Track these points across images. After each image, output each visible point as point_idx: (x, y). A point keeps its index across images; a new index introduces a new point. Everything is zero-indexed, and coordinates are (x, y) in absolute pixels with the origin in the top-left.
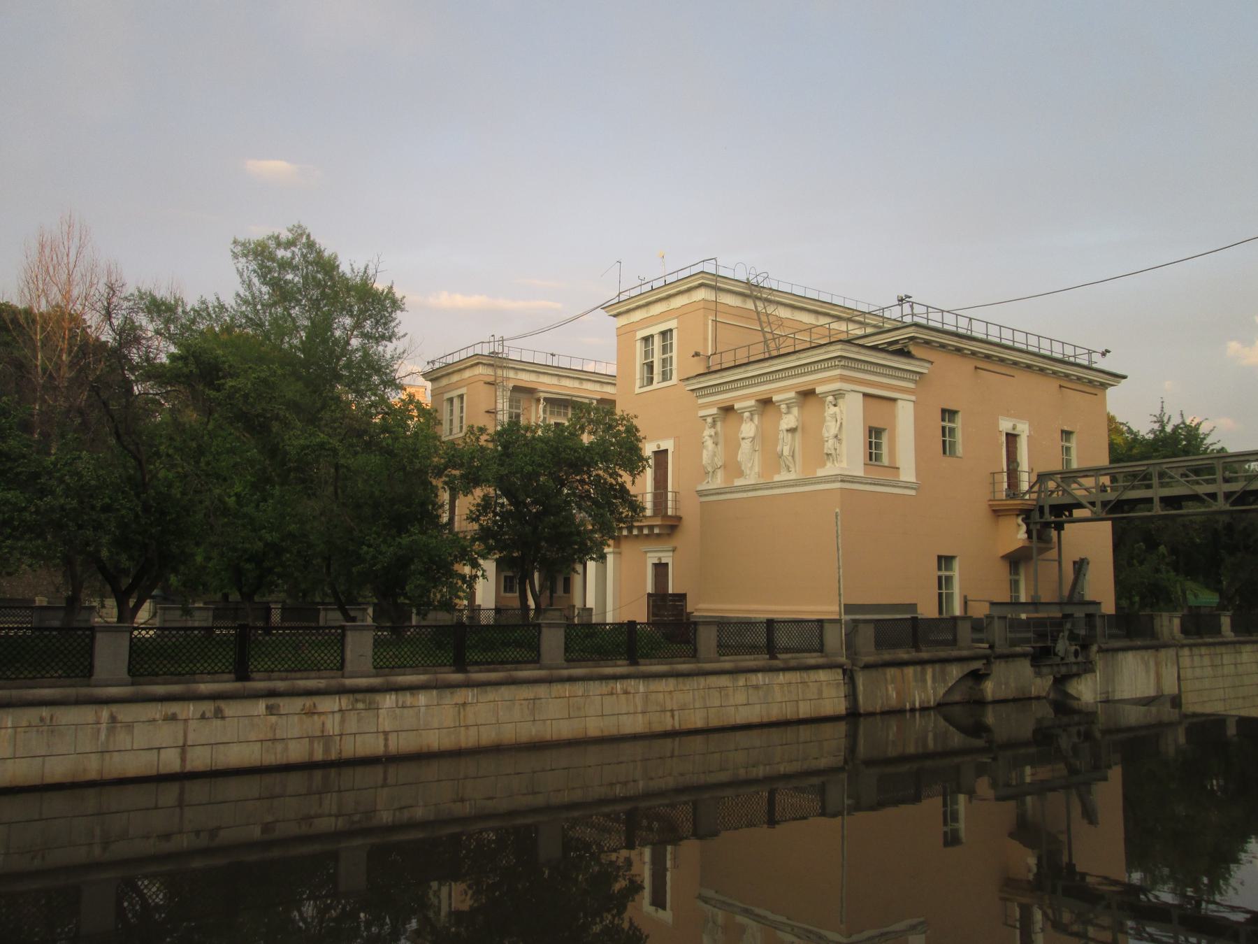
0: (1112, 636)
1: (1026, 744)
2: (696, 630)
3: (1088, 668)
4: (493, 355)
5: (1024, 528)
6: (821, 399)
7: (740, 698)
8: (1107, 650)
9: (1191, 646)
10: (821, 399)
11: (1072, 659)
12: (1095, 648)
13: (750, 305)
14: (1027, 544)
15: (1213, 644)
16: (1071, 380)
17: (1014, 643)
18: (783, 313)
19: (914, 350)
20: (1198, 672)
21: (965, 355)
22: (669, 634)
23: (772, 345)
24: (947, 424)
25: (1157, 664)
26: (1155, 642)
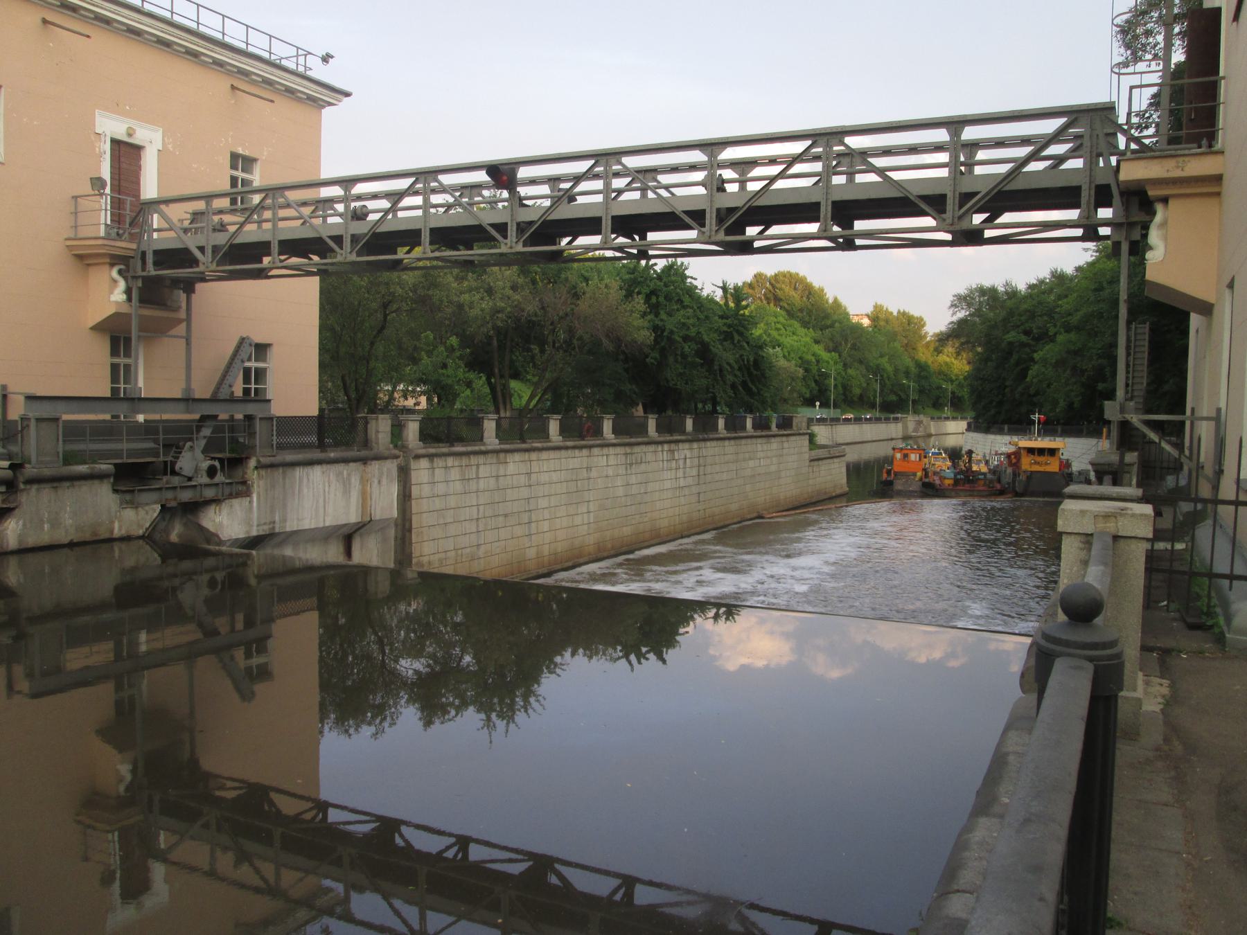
0: (281, 447)
1: (102, 607)
3: (242, 490)
5: (122, 285)
8: (272, 466)
9: (431, 457)
11: (205, 479)
12: (252, 463)
14: (125, 309)
15: (468, 454)
16: (254, 83)
17: (69, 459)
20: (441, 489)
21: (299, 100)
24: (240, 174)
25: (364, 481)
26: (364, 453)
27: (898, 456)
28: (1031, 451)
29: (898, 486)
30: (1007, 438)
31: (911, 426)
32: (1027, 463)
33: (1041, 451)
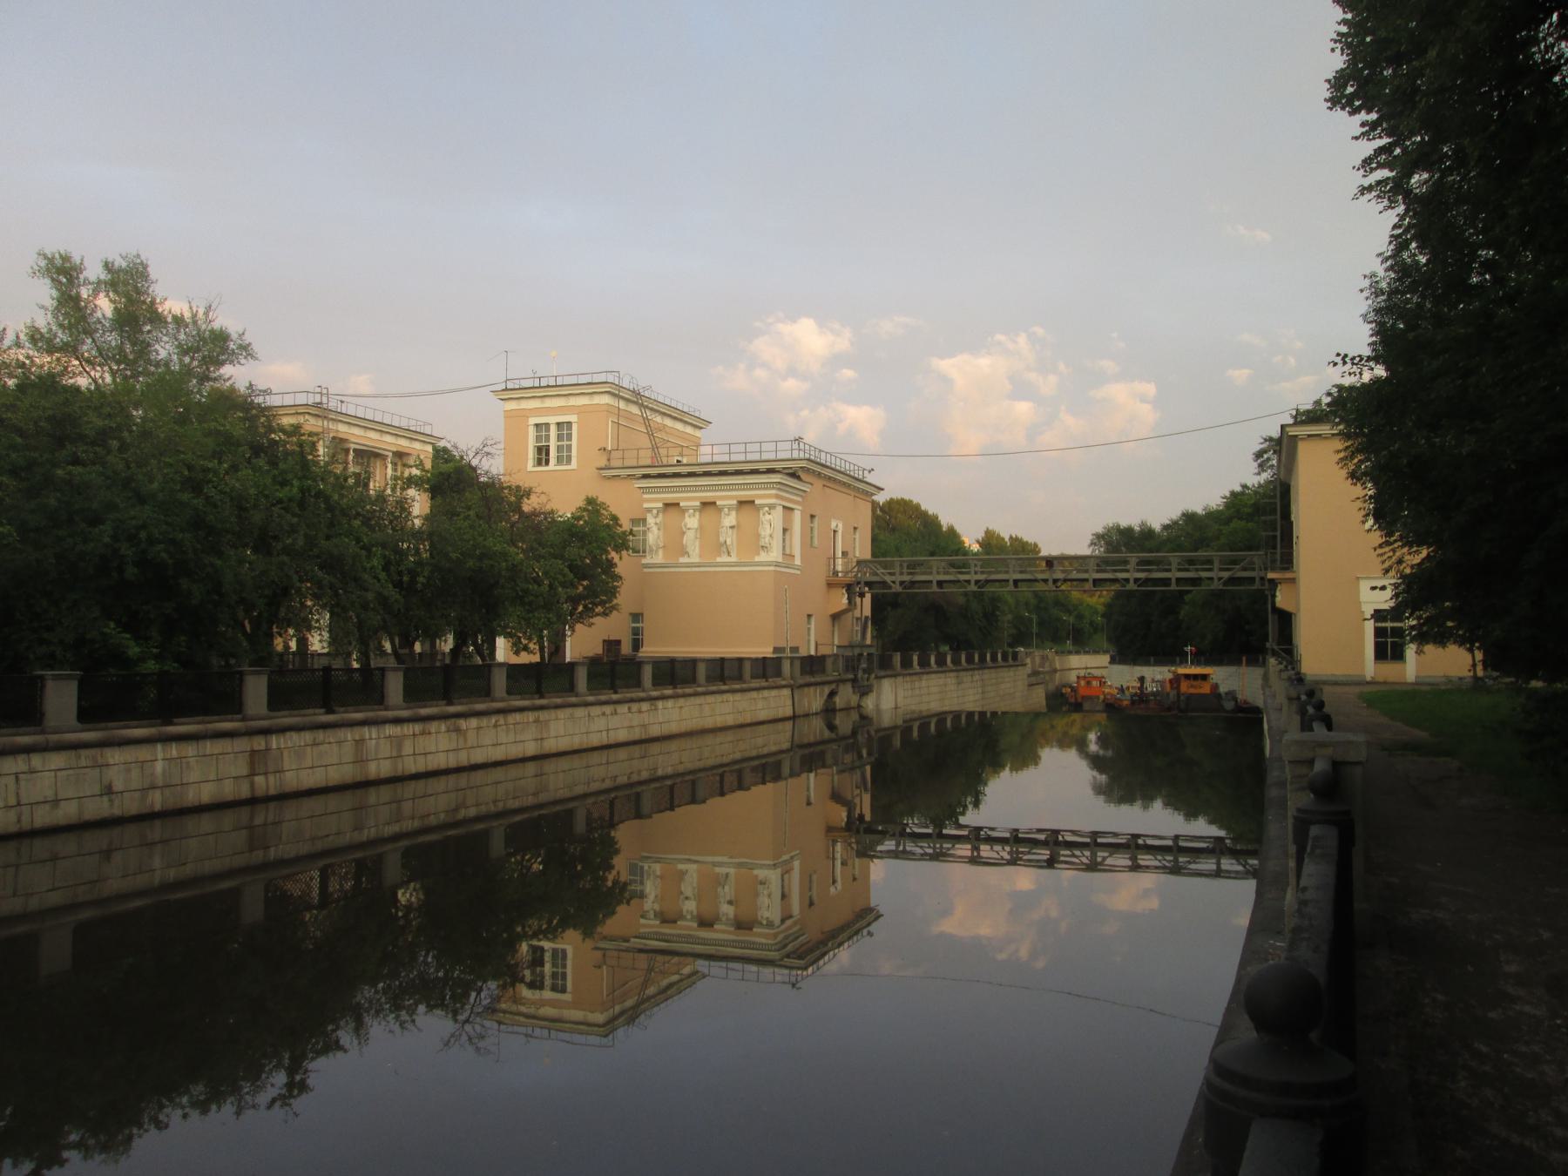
2: (241, 680)
4: (318, 405)
6: (758, 508)
7: (760, 705)
10: (758, 508)
13: (635, 410)
18: (668, 422)
19: (803, 476)
22: (616, 672)
23: (663, 452)
27: (1083, 683)
28: (1187, 677)
29: (1086, 706)
30: (1165, 669)
31: (1038, 660)
32: (1184, 687)
33: (1196, 677)
